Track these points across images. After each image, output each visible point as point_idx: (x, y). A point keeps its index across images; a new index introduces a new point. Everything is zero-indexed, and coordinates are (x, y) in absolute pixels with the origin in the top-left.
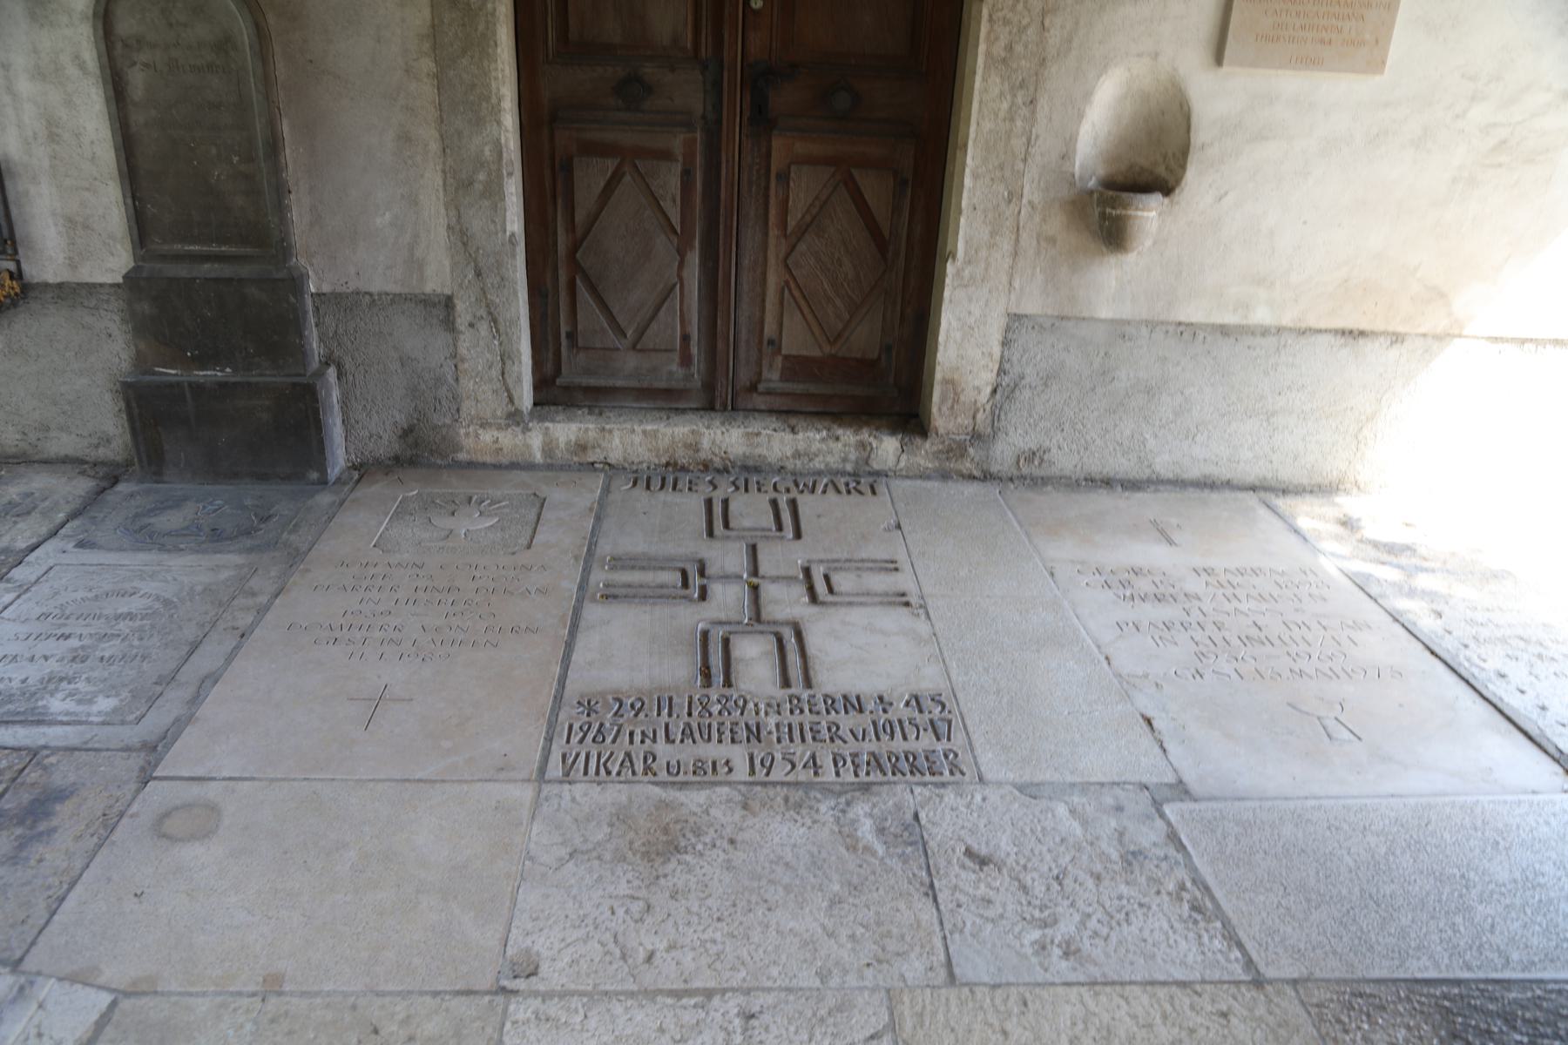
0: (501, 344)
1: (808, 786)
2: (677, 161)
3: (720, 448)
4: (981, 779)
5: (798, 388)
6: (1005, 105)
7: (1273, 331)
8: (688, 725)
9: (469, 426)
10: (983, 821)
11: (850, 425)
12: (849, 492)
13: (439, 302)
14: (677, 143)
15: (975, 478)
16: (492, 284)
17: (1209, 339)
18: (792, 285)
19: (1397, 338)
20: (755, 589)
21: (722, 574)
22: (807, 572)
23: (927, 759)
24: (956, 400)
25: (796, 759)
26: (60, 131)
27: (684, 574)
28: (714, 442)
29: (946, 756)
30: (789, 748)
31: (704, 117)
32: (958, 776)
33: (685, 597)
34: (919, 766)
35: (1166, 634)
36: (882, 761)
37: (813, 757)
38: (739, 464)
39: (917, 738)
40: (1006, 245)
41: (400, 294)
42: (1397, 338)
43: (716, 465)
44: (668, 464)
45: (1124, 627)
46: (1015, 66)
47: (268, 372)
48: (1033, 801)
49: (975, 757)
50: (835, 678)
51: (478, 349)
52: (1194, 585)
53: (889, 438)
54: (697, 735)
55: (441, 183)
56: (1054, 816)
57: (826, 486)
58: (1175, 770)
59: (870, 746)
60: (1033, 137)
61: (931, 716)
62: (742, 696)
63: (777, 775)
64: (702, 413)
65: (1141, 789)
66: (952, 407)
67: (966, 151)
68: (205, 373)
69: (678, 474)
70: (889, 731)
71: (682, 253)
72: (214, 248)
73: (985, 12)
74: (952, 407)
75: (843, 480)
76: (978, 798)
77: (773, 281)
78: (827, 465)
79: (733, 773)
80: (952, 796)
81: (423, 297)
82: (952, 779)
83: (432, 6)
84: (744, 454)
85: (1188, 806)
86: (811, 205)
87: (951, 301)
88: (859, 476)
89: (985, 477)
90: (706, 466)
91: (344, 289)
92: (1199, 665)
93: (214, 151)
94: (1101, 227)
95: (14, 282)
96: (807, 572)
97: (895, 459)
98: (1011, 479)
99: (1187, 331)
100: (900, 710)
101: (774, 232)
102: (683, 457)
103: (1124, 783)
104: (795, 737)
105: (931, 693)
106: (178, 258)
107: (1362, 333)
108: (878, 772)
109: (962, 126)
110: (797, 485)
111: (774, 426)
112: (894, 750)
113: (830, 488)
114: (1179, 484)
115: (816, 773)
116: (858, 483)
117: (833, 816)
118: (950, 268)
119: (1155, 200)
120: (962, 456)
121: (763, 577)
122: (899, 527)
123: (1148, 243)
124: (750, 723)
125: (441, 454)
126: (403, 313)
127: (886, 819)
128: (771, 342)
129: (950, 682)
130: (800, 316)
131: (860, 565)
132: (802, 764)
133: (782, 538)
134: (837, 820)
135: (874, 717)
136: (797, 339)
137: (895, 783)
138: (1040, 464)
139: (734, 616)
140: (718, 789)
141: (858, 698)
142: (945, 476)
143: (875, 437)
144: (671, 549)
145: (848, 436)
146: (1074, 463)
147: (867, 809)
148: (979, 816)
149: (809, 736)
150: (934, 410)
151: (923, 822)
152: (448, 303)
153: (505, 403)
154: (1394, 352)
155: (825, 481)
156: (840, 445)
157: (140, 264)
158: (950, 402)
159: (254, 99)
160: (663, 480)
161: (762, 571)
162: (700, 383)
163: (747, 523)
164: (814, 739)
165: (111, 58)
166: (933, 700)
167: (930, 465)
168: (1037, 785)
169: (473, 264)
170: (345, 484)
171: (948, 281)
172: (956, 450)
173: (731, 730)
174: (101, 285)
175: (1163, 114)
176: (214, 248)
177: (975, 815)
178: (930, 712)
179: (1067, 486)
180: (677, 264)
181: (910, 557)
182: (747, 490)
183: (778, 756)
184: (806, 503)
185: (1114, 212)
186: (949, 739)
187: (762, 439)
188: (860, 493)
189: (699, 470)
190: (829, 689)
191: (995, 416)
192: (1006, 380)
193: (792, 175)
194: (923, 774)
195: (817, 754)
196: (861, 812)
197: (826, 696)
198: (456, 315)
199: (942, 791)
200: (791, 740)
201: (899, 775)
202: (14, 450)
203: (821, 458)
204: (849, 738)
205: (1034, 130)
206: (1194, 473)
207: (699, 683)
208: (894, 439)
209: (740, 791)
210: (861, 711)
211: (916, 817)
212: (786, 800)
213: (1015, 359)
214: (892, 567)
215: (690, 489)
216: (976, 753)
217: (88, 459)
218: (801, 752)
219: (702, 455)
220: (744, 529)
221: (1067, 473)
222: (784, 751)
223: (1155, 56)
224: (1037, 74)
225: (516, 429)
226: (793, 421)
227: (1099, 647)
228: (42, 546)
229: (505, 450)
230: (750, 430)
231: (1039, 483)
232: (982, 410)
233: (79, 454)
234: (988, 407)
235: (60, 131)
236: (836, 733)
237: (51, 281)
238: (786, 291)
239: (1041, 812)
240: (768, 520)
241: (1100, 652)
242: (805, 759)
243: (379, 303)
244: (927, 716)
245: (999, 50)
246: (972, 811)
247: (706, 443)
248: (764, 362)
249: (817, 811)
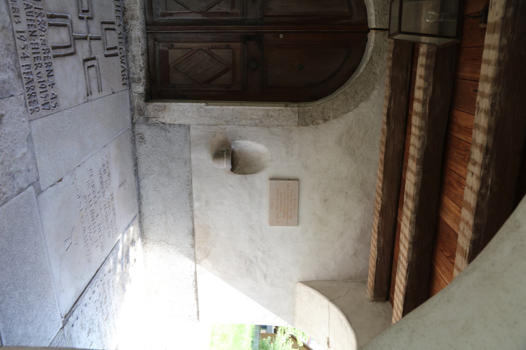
1: (17, 54)
2: (231, 10)
3: (133, 28)
4: (31, 120)
5: (157, 56)
6: (255, 117)
7: (192, 209)
8: (31, 7)
10: (15, 121)
11: (146, 75)
12: (123, 75)
14: (237, 10)
15: (132, 120)
17: (188, 190)
18: (192, 52)
19: (193, 246)
20: (85, 38)
21: (89, 25)
22: (94, 59)
23: (35, 101)
24: (159, 111)
25: (26, 50)
27: (87, 11)
28: (135, 25)
29: (37, 108)
30: (30, 48)
31: (246, 19)
32: (31, 112)
33: (79, 10)
34: (31, 98)
35: (90, 186)
36: (31, 83)
37: (27, 57)
38: (128, 35)
39: (42, 97)
40: (212, 122)
42: (193, 246)
43: (126, 26)
44: (125, 8)
45: (91, 171)
46: (267, 119)
48: (26, 139)
49: (38, 118)
50: (58, 65)
52: (108, 194)
53: (143, 89)
54: (28, 10)
56: (22, 147)
57: (124, 67)
58: (46, 190)
59: (36, 80)
60: (246, 127)
61: (50, 102)
62: (46, 30)
63: (19, 42)
64: (145, 21)
65: (37, 178)
66: (156, 110)
67: (240, 106)
69: (122, 12)
70: (42, 86)
71: (201, 12)
73: (282, 108)
74: (156, 110)
75: (126, 73)
76: (24, 119)
77: (193, 45)
78: (131, 67)
79: (16, 24)
80: (22, 109)
82: (29, 110)
84: (132, 37)
85: (34, 195)
86: (220, 57)
87: (192, 106)
88: (128, 79)
89: (133, 123)
90: (126, 23)
92: (82, 197)
94: (220, 151)
96: (94, 59)
97: (136, 91)
98: (133, 132)
99: (189, 182)
100: (51, 91)
101: (210, 45)
102: (128, 14)
103: (38, 172)
104: (34, 50)
105: (58, 103)
107: (194, 235)
108: (27, 82)
109: (248, 104)
110: (123, 56)
111: (143, 47)
112: (35, 88)
113: (123, 69)
114: (139, 188)
115: (22, 57)
116: (126, 79)
117: (6, 63)
118: (203, 104)
119: (229, 166)
120: (140, 115)
121: (90, 42)
122: (113, 93)
123: (216, 166)
124: (37, 33)
127: (9, 84)
128: (172, 46)
129: (63, 110)
130: (183, 55)
131: (99, 78)
132: (24, 52)
133: (104, 50)
134: (5, 65)
135: (47, 81)
136: (174, 55)
137: (23, 88)
138: (140, 141)
139: (75, 29)
140: (8, 17)
141: (52, 75)
142: (132, 109)
143: (143, 84)
144: (96, 7)
145: (142, 74)
146: (142, 153)
147: (12, 77)
148: (17, 120)
149: (35, 55)
150: (155, 104)
151: (11, 98)
154: (189, 246)
155: (125, 67)
156: (139, 72)
158: (158, 109)
160: (119, 6)
161: (92, 41)
162: (156, 20)
163: (108, 37)
164: (35, 58)
166: (56, 103)
167: (135, 104)
168: (32, 141)
171: (199, 104)
172: (141, 113)
173: (32, 25)
175: (255, 165)
177: (17, 118)
178: (52, 102)
179: (133, 152)
180: (197, 11)
181: (104, 96)
182: (119, 38)
183: (26, 43)
184: (116, 60)
185: (225, 154)
186: (43, 109)
187: (138, 43)
188: (123, 80)
189: (124, 20)
190: (54, 64)
191: (154, 124)
192: (168, 127)
193: (229, 50)
194: (29, 98)
195: (29, 58)
196: (10, 74)
197: (51, 63)
199: (24, 106)
200: (33, 49)
201: (27, 90)
203: (133, 65)
204: (38, 71)
205: (248, 127)
206: (143, 192)
207: (48, 13)
208: (143, 91)
209: (9, 26)
210: (48, 76)
211: (12, 96)
212: (9, 45)
213: (175, 129)
214: (100, 90)
215: (117, 16)
216: (40, 119)
218: (29, 52)
219: (130, 21)
220: (106, 36)
221: (138, 151)
222: (28, 45)
223: (271, 161)
224: (264, 126)
226: (145, 54)
227: (83, 163)
230: (141, 39)
231: (133, 142)
232: (157, 120)
234: (158, 122)
236: (38, 66)
238: (190, 50)
239: (23, 143)
240: (110, 45)
241: (81, 163)
242: (26, 53)
244: (50, 101)
245: (271, 113)
246: (18, 117)
247: (134, 22)
248: (165, 43)
249: (7, 57)
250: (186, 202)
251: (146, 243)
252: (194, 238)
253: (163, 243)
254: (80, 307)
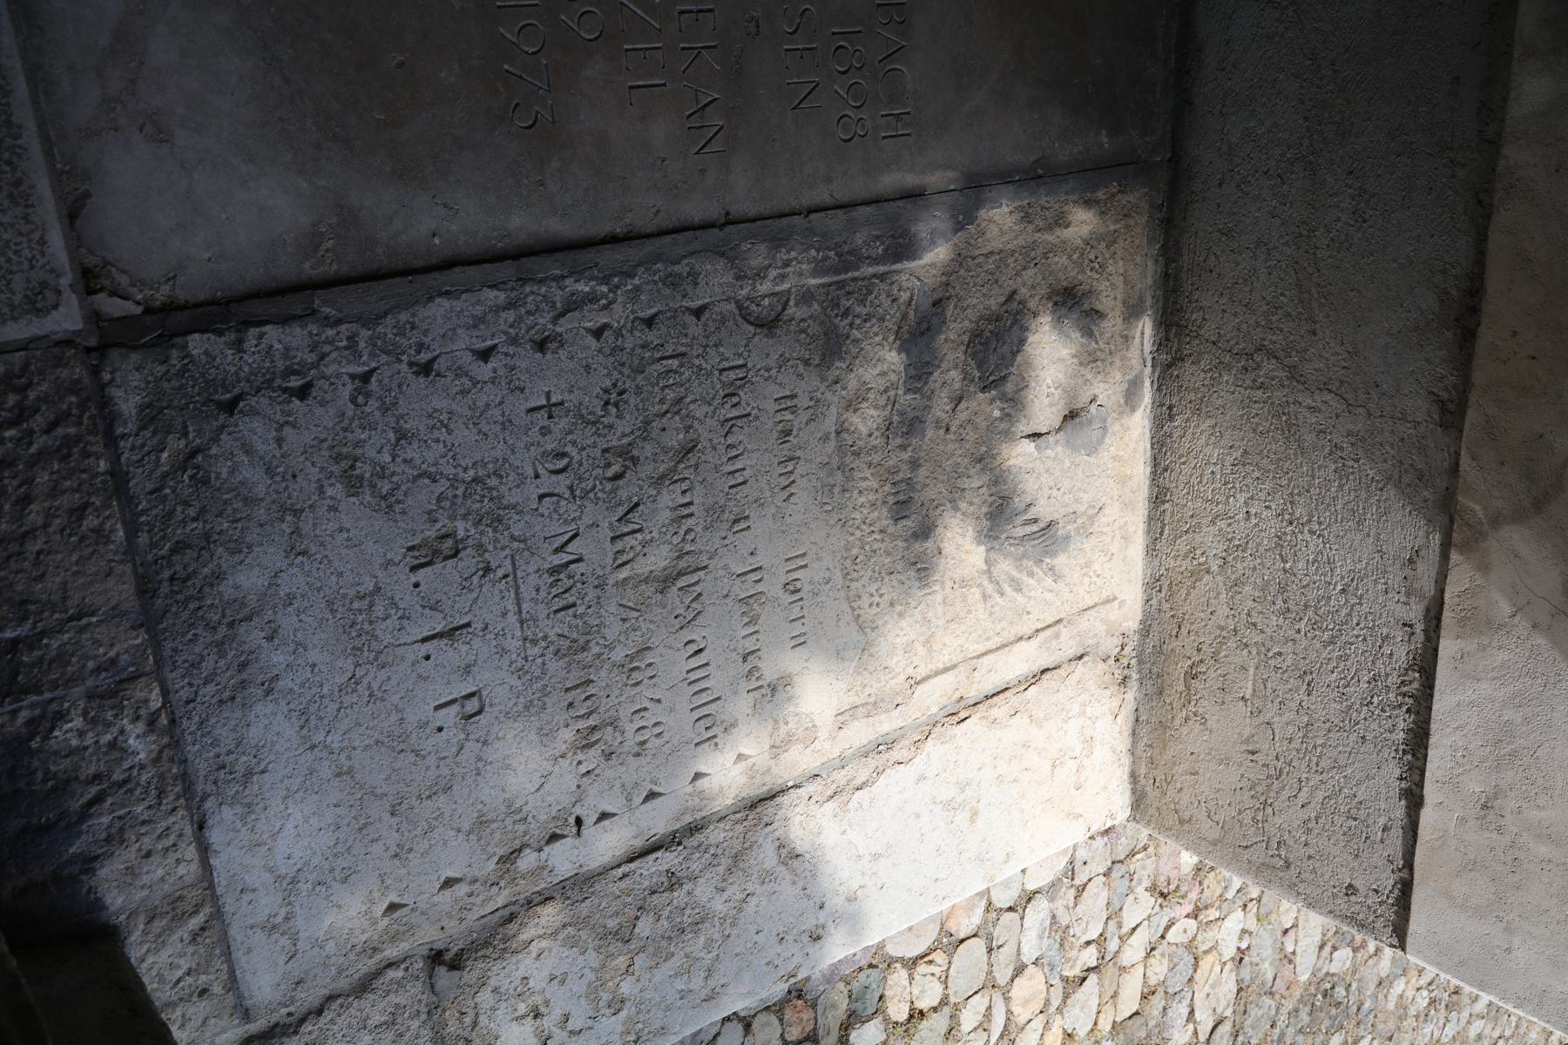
19: (1451, 414)
42: (1451, 414)
107: (1467, 336)
154: (1419, 407)
250: (1458, 78)
251: (1178, 359)
252: (1470, 357)
253: (1269, 366)
254: (338, 333)
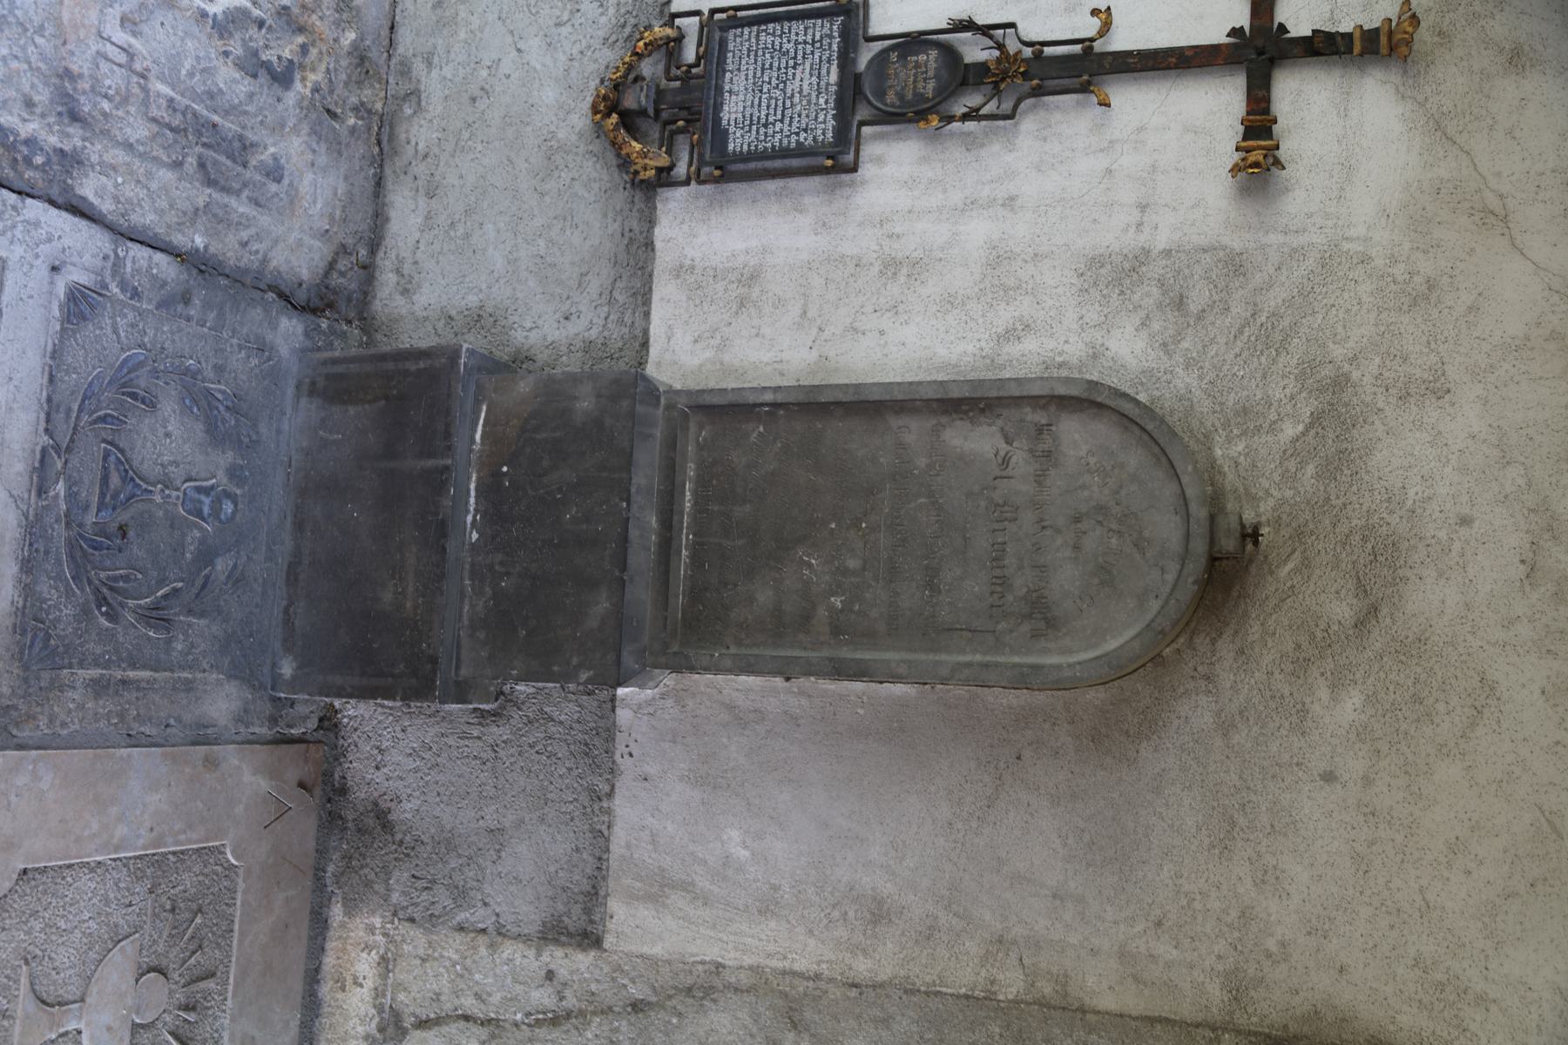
0: (516, 1025)
9: (385, 935)
13: (592, 922)
16: (617, 1030)
26: (903, 279)
41: (608, 850)
47: (466, 608)
51: (509, 980)
55: (797, 967)
68: (473, 493)
72: (686, 537)
81: (602, 893)
83: (1121, 1016)
91: (620, 748)
93: (853, 563)
95: (653, 172)
106: (671, 471)
125: (342, 874)
126: (577, 850)
152: (590, 939)
153: (418, 1011)
157: (663, 401)
159: (943, 657)
165: (1017, 401)
169: (654, 999)
170: (273, 720)
174: (647, 315)
176: (686, 537)
198: (569, 951)
202: (403, 136)
217: (381, 254)
225: (374, 1025)
228: (83, 224)
229: (340, 995)
233: (388, 242)
235: (903, 279)
237: (657, 231)
243: (596, 807)
